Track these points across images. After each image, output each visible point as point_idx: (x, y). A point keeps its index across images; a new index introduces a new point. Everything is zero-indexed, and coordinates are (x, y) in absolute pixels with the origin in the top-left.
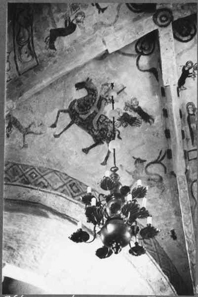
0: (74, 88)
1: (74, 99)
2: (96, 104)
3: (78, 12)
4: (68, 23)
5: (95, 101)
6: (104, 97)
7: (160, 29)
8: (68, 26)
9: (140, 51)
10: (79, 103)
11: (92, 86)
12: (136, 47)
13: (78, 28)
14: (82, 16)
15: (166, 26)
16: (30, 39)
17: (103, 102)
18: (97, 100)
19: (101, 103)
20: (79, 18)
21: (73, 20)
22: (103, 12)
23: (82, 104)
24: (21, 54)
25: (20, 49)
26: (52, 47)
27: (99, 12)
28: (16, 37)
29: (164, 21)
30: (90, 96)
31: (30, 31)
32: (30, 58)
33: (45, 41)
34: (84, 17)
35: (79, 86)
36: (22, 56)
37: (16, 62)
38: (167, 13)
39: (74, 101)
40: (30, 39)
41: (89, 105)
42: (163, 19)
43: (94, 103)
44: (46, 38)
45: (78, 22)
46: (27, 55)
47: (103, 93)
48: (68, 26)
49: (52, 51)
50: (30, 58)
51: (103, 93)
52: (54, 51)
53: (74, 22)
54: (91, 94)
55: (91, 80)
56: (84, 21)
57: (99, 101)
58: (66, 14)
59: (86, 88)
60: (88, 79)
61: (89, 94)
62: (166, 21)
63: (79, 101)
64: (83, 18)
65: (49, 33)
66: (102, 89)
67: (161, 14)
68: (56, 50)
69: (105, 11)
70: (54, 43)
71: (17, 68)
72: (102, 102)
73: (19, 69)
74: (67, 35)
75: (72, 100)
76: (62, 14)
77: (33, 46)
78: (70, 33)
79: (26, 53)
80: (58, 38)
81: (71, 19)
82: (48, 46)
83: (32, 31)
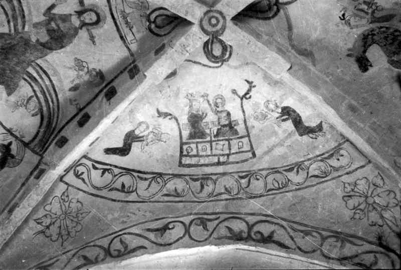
0: (371, 71)
1: (387, 65)
2: (386, 24)
3: (266, 111)
4: (283, 118)
5: (381, 27)
6: (369, 16)
7: (228, 19)
8: (287, 117)
9: (275, 7)
10: (394, 53)
11: (361, 43)
12: (273, 17)
13: (285, 104)
14: (269, 104)
15: (221, 13)
16: (319, 158)
17: (378, 14)
18: (378, 25)
19: (382, 17)
20: (272, 106)
21: (278, 113)
22: (252, 82)
23: (393, 48)
24: (341, 167)
25: (336, 169)
26: (320, 127)
27: (255, 86)
28: (323, 180)
29: (217, 19)
30: (375, 37)
31: (310, 162)
32: (342, 152)
33: (316, 138)
34: (268, 101)
35: (364, 64)
36: (343, 165)
37: (354, 171)
38: (205, 23)
39: (391, 64)
40: (319, 158)
41: (392, 34)
42: (214, 21)
43: (387, 28)
44: (312, 138)
45: (277, 107)
46: (341, 158)
47: (364, 21)
48: (287, 117)
49: (325, 126)
50: (342, 152)
51: (364, 21)
52: (323, 123)
53: (280, 110)
54: (372, 38)
55: (349, 50)
56: (273, 99)
57: (379, 22)
58: (275, 123)
59: (365, 52)
60: (348, 55)
61: (374, 42)
62: (213, 17)
63: (390, 54)
64: (270, 102)
65: (305, 137)
66: (357, 26)
67: (210, 29)
68: (321, 122)
69: (250, 80)
70: (314, 127)
71: (362, 167)
72: (378, 16)
73: (362, 164)
74: (298, 115)
75: (391, 66)
76: (276, 128)
77: (327, 152)
78: (294, 111)
79: (338, 160)
80: (307, 124)
81: (278, 115)
82: (321, 134)
83: (309, 160)
